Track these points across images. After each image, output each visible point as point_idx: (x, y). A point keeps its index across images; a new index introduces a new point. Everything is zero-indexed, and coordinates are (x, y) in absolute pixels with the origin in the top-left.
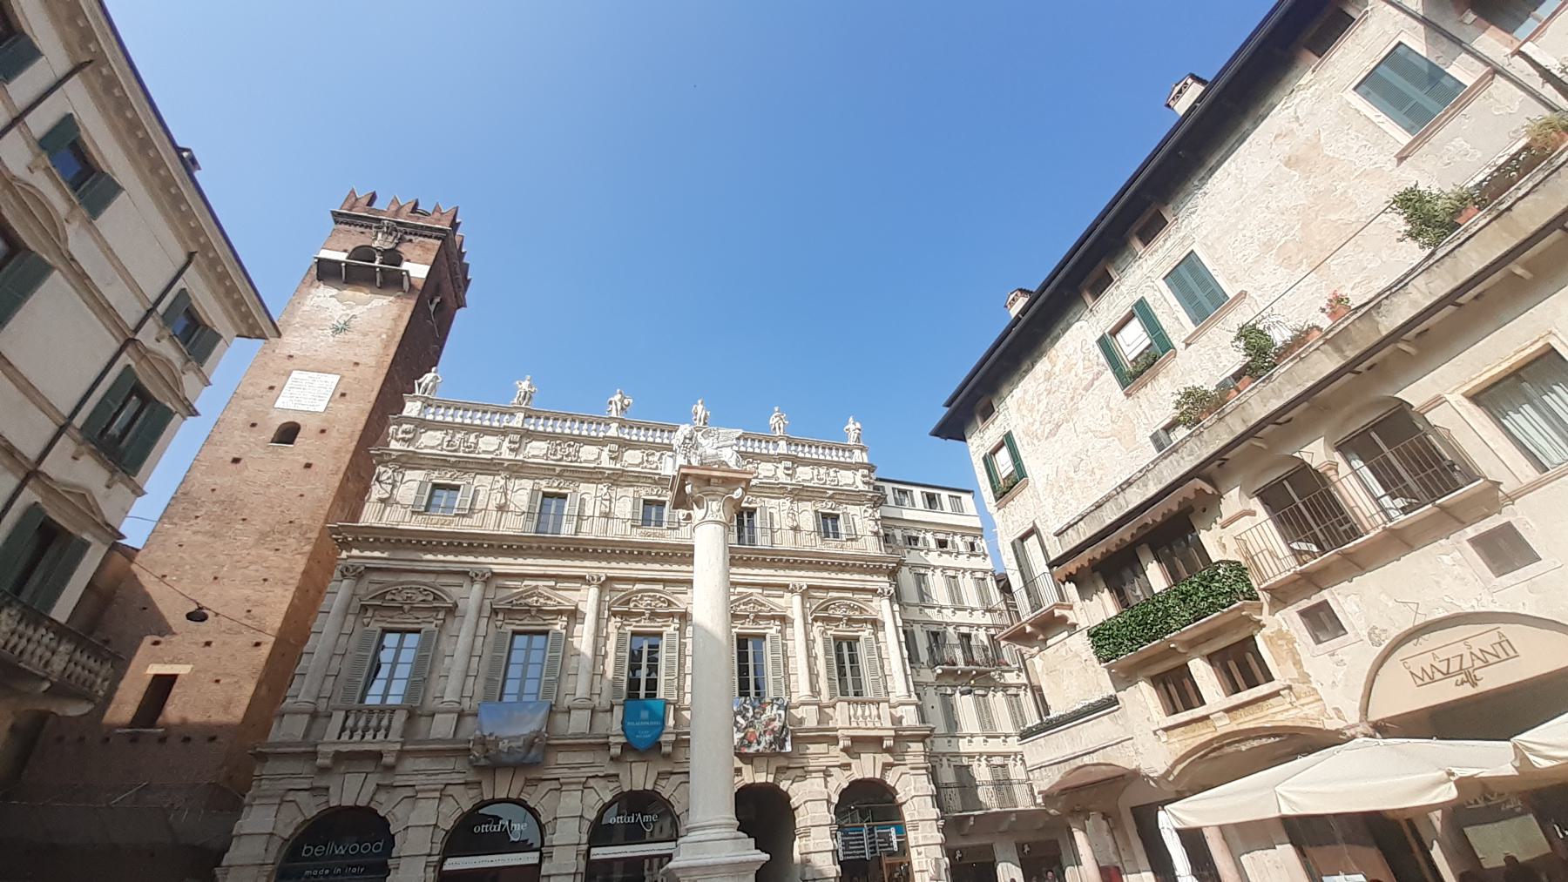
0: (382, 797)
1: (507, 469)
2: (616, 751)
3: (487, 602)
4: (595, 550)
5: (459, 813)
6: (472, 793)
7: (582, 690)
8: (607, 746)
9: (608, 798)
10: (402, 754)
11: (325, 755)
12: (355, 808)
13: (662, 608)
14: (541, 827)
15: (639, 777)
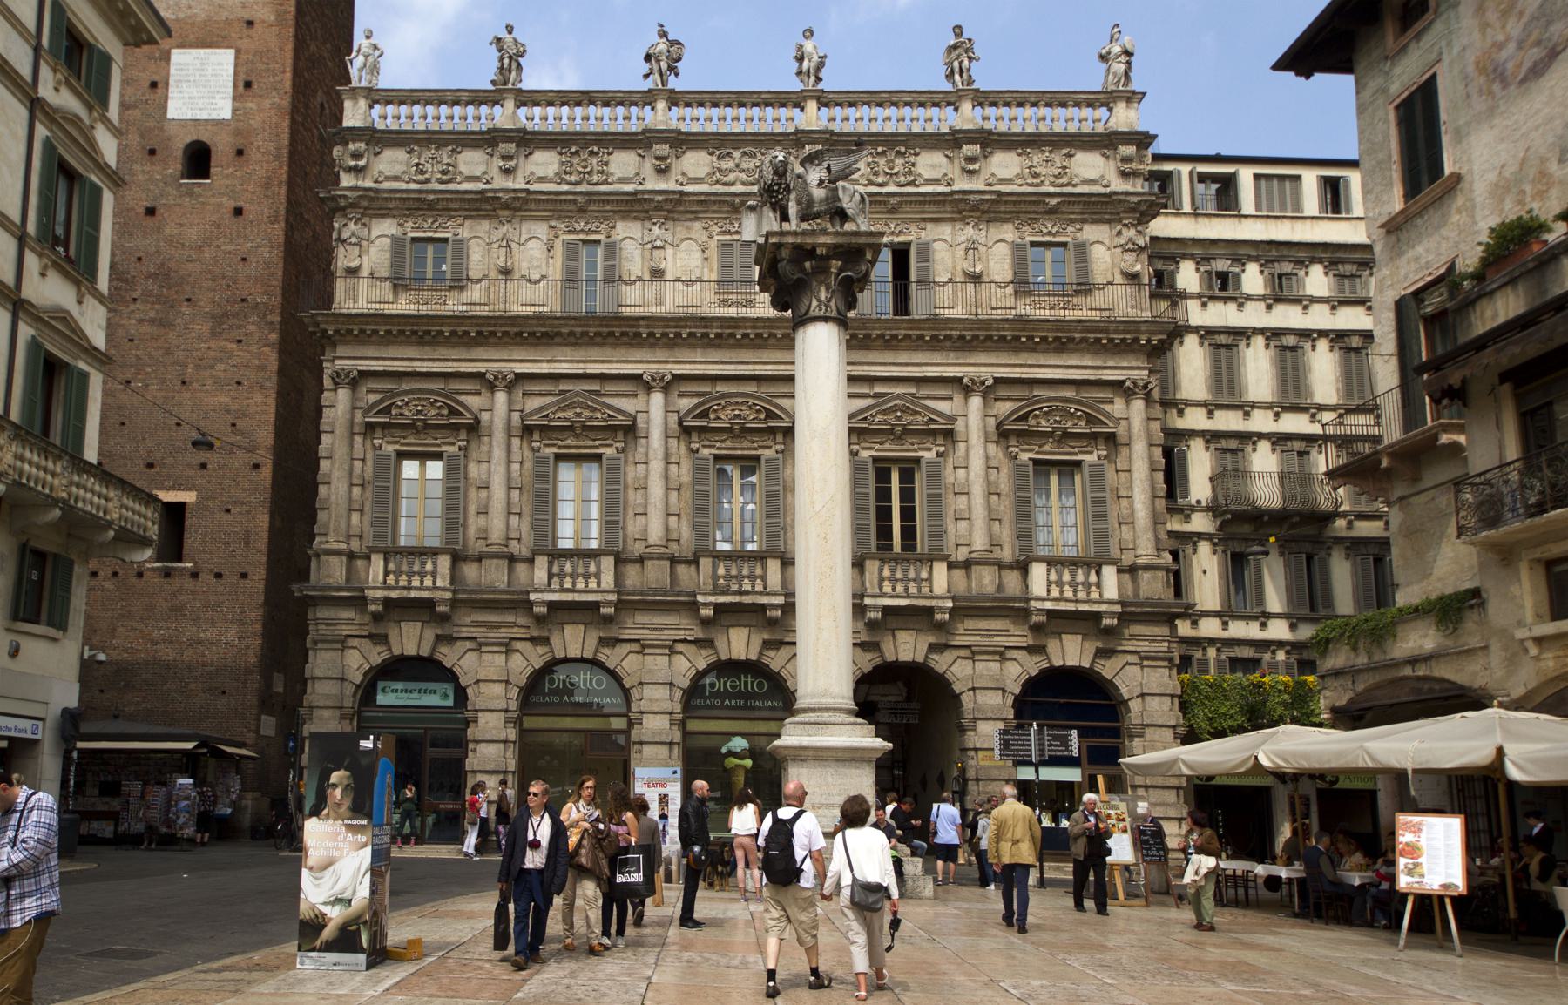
0: (444, 649)
1: (506, 206)
2: (707, 612)
3: (516, 416)
4: (651, 335)
5: (529, 670)
6: (541, 650)
7: (656, 533)
8: (693, 606)
9: (702, 665)
10: (454, 603)
11: (375, 601)
12: (418, 659)
13: (753, 420)
14: (626, 692)
15: (739, 643)
